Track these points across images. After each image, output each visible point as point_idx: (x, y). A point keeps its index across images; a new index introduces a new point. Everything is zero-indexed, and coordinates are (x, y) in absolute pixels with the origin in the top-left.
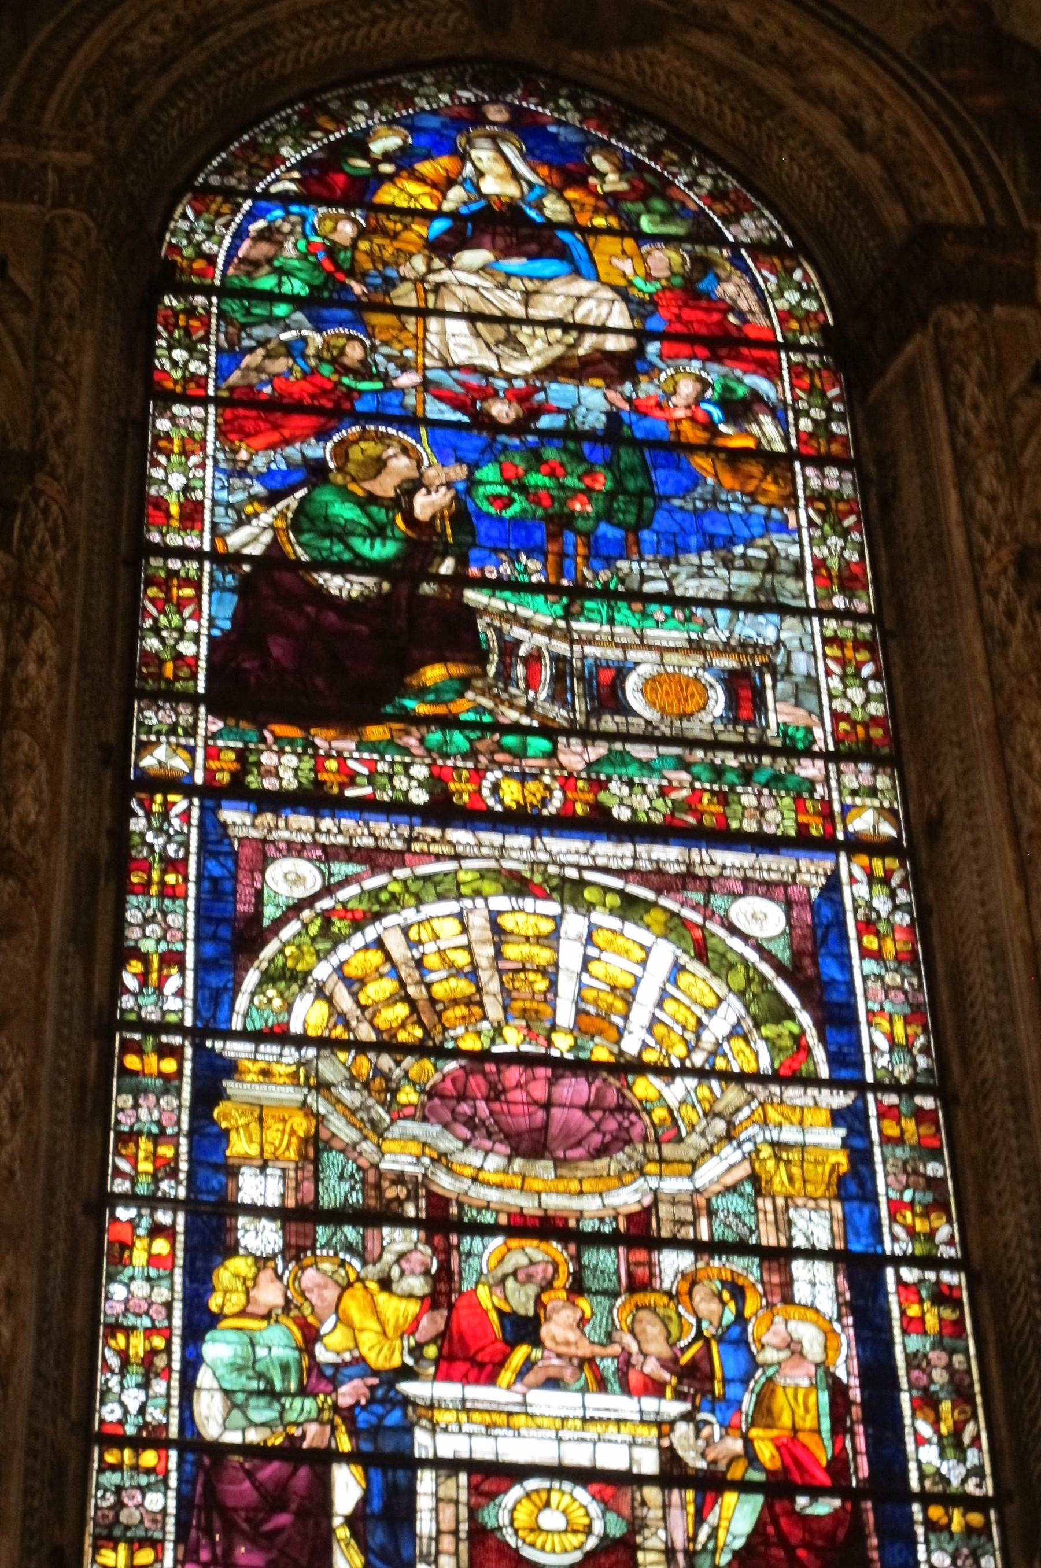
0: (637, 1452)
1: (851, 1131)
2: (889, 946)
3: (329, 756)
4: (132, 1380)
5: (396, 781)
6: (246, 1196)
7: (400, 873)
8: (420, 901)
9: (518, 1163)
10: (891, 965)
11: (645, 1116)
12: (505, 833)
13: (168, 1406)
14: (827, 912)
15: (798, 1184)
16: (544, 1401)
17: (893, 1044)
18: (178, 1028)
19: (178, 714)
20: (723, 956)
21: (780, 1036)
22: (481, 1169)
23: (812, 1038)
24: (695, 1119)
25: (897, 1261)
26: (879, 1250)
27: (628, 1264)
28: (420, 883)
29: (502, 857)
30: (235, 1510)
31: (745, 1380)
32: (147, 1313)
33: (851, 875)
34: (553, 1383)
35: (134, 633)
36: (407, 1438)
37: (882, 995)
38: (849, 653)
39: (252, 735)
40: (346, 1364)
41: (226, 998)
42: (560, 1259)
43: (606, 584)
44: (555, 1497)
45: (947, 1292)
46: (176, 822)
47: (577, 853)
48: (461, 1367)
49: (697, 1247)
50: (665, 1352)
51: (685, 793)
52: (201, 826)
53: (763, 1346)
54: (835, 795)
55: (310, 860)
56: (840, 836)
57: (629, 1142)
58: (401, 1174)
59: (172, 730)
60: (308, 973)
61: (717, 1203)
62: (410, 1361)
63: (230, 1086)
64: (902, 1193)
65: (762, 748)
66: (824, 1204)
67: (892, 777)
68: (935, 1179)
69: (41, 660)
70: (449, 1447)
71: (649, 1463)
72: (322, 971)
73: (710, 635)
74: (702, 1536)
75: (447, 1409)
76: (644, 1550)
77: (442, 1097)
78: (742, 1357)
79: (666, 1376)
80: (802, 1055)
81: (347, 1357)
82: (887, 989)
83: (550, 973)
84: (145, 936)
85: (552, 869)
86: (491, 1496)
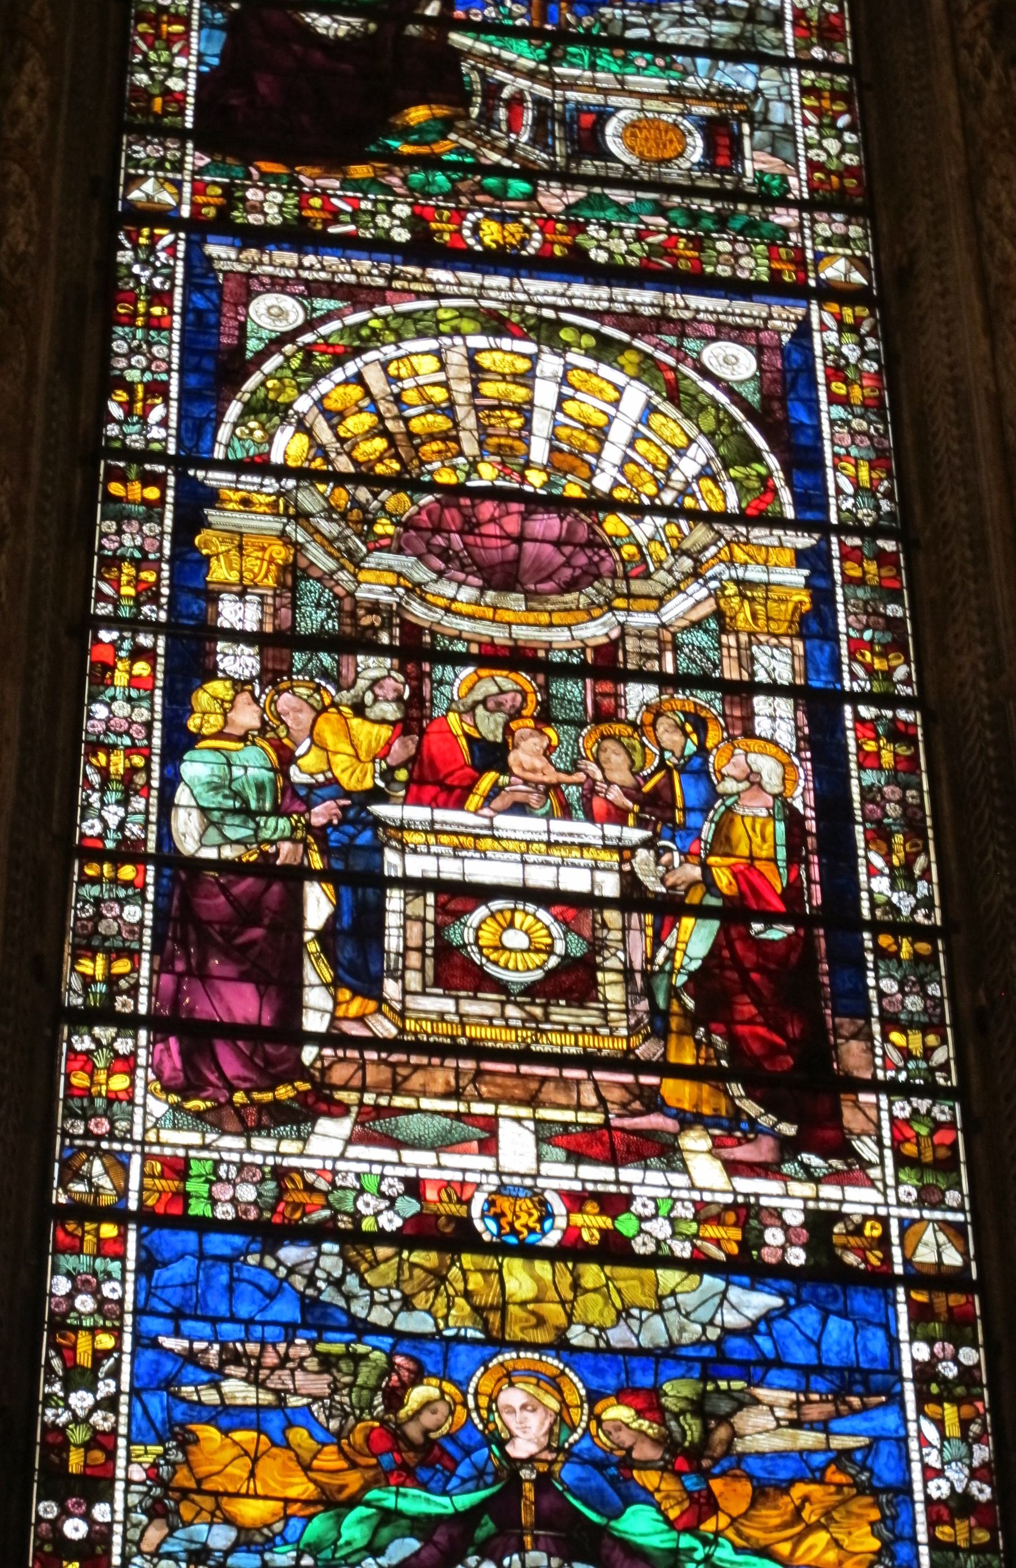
0: (599, 876)
1: (814, 571)
2: (856, 393)
3: (314, 194)
4: (111, 797)
5: (379, 220)
6: (223, 623)
7: (382, 310)
8: (400, 338)
9: (490, 596)
10: (858, 411)
11: (614, 551)
12: (484, 273)
13: (147, 822)
15: (762, 622)
16: (509, 824)
17: (858, 487)
18: (161, 457)
19: (166, 149)
20: (694, 398)
21: (748, 477)
22: (454, 600)
23: (779, 479)
24: (663, 556)
25: (856, 698)
27: (595, 694)
28: (400, 320)
29: (481, 297)
30: (210, 923)
31: (705, 809)
32: (127, 733)
33: (822, 322)
34: (520, 808)
35: (125, 68)
36: (377, 857)
37: (848, 440)
38: (826, 104)
39: (239, 171)
40: (319, 785)
41: (209, 429)
42: (528, 688)
43: (588, 29)
44: (519, 917)
45: (902, 727)
46: (162, 256)
47: (554, 294)
48: (430, 791)
49: (661, 680)
50: (629, 780)
51: (662, 237)
52: (187, 260)
53: (723, 776)
54: (808, 243)
55: (292, 295)
56: (812, 283)
57: (598, 577)
58: (377, 603)
59: (160, 165)
60: (289, 405)
61: (684, 638)
62: (381, 784)
63: (213, 515)
64: (861, 631)
65: (738, 195)
66: (786, 641)
67: (864, 227)
68: (895, 618)
69: (32, 93)
70: (417, 866)
71: (610, 886)
72: (303, 404)
73: (690, 82)
74: (660, 958)
75: (417, 831)
76: (605, 970)
77: (418, 529)
79: (630, 804)
80: (769, 497)
81: (321, 778)
82: (853, 433)
83: (525, 410)
84: (131, 367)
85: (530, 309)
86: (458, 915)
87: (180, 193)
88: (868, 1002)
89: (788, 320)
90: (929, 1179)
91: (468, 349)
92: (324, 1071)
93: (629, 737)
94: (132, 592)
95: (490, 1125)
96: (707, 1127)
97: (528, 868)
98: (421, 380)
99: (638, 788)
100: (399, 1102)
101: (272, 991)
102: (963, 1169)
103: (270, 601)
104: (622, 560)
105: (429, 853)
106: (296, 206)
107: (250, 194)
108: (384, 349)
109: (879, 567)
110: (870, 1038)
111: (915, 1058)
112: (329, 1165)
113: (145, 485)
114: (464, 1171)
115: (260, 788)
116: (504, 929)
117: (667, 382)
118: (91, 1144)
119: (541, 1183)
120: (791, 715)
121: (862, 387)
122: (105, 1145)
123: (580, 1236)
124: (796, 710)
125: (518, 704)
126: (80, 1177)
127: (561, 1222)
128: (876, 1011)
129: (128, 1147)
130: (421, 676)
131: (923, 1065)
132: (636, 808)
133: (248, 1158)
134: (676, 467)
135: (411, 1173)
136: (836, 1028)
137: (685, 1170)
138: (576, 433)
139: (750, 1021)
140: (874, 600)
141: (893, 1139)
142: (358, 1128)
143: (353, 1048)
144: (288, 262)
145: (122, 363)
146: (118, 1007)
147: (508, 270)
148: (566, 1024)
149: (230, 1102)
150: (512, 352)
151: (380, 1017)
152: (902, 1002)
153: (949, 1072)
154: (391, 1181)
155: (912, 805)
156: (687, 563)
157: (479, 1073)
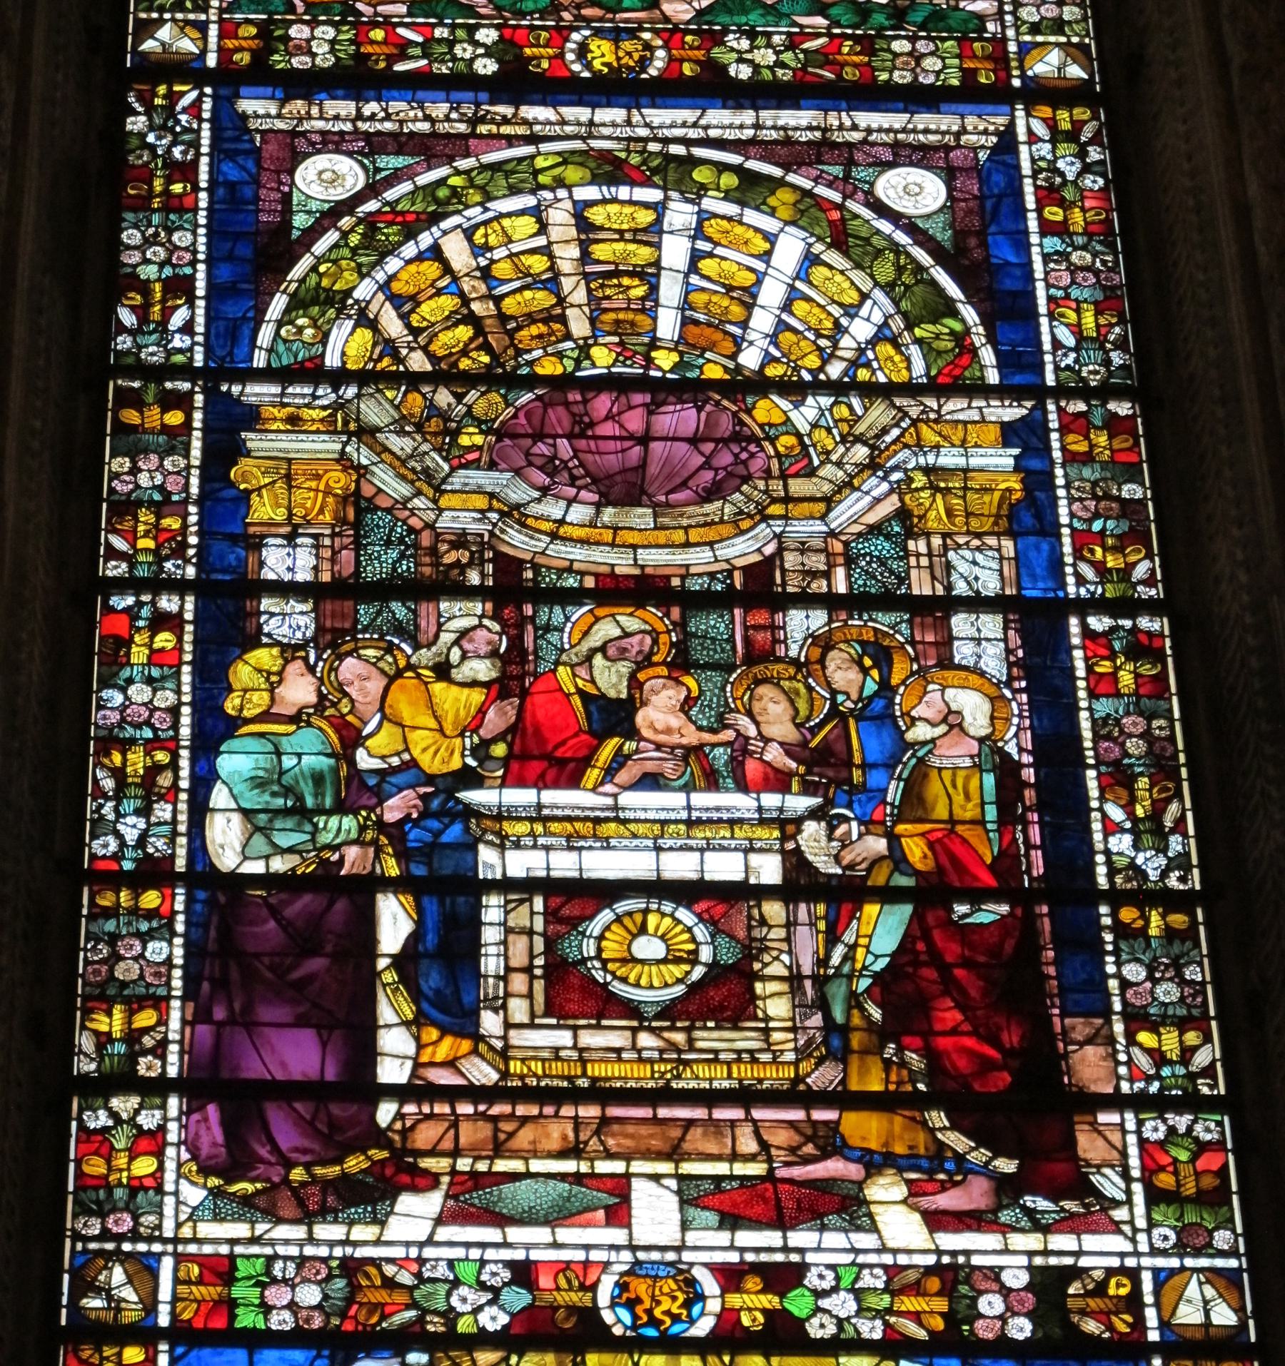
0: (755, 859)
1: (1027, 451)
2: (1077, 217)
3: (375, 25)
4: (129, 805)
5: (458, 50)
7: (463, 164)
8: (489, 197)
9: (608, 514)
10: (1080, 240)
11: (766, 444)
12: (594, 106)
13: (175, 834)
14: (999, 179)
18: (187, 371)
20: (867, 241)
21: (938, 336)
22: (561, 522)
23: (978, 336)
25: (1083, 607)
26: (1061, 594)
27: (746, 628)
29: (591, 136)
30: (257, 956)
31: (890, 765)
33: (1030, 132)
34: (651, 781)
36: (469, 857)
37: (1066, 279)
40: (394, 770)
41: (246, 332)
42: (661, 628)
44: (652, 920)
45: (1144, 639)
47: (684, 125)
48: (536, 767)
49: (830, 602)
50: (791, 734)
51: (822, 41)
53: (914, 720)
54: (1011, 33)
55: (350, 154)
56: (1016, 83)
57: (747, 479)
58: (464, 533)
60: (348, 293)
62: (472, 762)
63: (253, 440)
64: (1090, 521)
66: (992, 541)
70: (521, 864)
71: (769, 870)
72: (364, 290)
74: (836, 959)
75: (519, 819)
78: (887, 737)
79: (794, 765)
80: (965, 360)
81: (395, 761)
82: (1073, 270)
83: (650, 275)
84: (146, 261)
85: (654, 147)
86: (575, 923)
87: (205, 38)
88: (1108, 995)
89: (985, 132)
90: (1191, 1217)
91: (575, 203)
92: (405, 1132)
93: (790, 678)
94: (150, 544)
95: (620, 1187)
96: (900, 1170)
97: (663, 856)
98: (516, 248)
99: (804, 744)
100: (501, 1166)
101: (337, 1034)
102: (1235, 1199)
103: (327, 542)
104: (778, 455)
105: (535, 847)
106: (352, 42)
107: (293, 31)
108: (467, 213)
109: (1111, 437)
110: (1111, 1041)
111: (1171, 1063)
112: (414, 1253)
113: (165, 410)
114: (587, 1247)
115: (318, 779)
116: (634, 936)
117: (831, 223)
118: (110, 1246)
119: (687, 1256)
120: (1000, 635)
121: (1083, 210)
122: (127, 1247)
123: (739, 1320)
124: (1006, 629)
125: (646, 649)
126: (98, 1291)
127: (714, 1306)
128: (1117, 1006)
129: (157, 1247)
130: (521, 622)
131: (1180, 1070)
132: (802, 769)
133: (309, 1251)
134: (846, 331)
135: (519, 1255)
136: (1065, 1032)
137: (874, 1229)
138: (715, 299)
139: (954, 1032)
140: (1104, 479)
141: (1144, 1168)
142: (451, 1203)
143: (442, 1101)
144: (343, 113)
145: (135, 257)
146: (142, 1070)
147: (624, 100)
148: (716, 1052)
149: (286, 1181)
150: (631, 202)
151: (477, 1060)
152: (1152, 992)
153: (1215, 1078)
154: (493, 1267)
155: (1159, 738)
156: (861, 452)
157: (604, 1122)
